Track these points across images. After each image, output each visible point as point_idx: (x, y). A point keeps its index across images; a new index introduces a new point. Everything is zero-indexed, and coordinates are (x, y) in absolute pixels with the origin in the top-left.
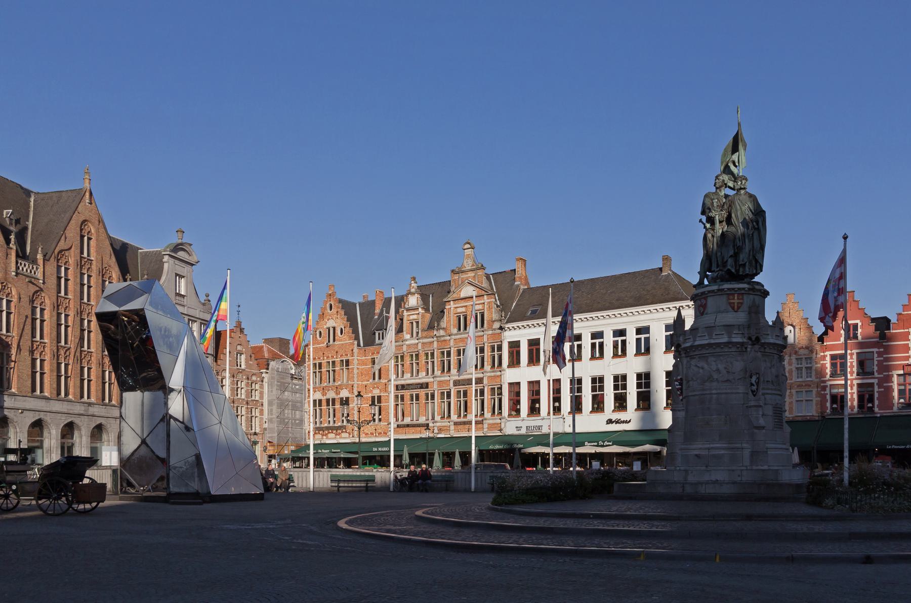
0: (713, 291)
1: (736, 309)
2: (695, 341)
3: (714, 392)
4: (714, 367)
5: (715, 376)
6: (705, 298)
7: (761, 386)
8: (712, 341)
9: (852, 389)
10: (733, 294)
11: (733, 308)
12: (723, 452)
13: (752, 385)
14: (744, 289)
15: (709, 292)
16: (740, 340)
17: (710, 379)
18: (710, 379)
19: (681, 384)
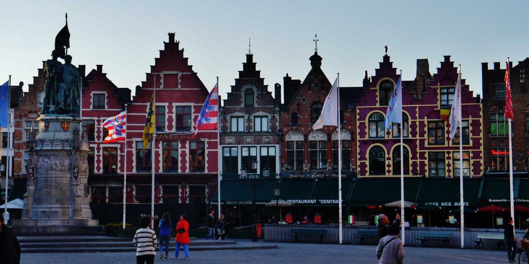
0: (53, 119)
1: (65, 130)
2: (42, 147)
3: (53, 176)
4: (54, 162)
5: (54, 167)
6: (48, 123)
7: (79, 174)
8: (54, 148)
9: (98, 152)
10: (64, 122)
11: (64, 130)
12: (58, 210)
13: (75, 173)
14: (70, 120)
15: (51, 119)
16: (68, 148)
17: (51, 169)
18: (51, 169)
19: (33, 170)
